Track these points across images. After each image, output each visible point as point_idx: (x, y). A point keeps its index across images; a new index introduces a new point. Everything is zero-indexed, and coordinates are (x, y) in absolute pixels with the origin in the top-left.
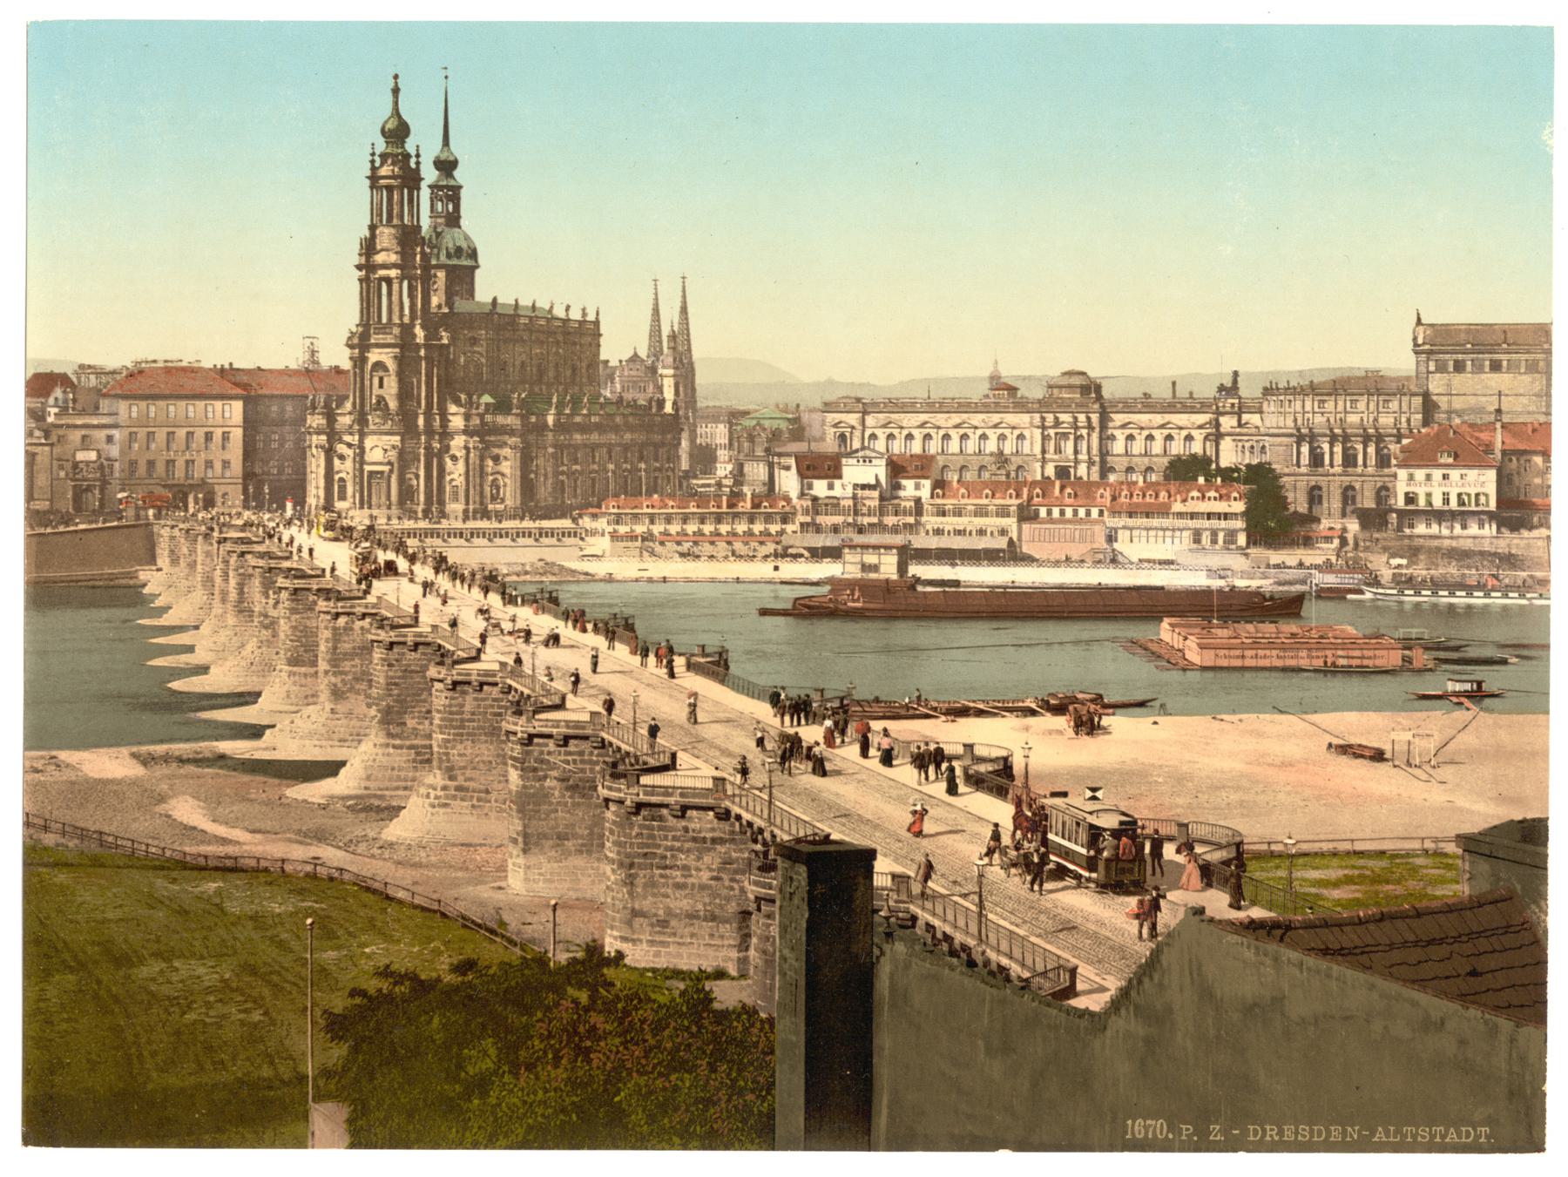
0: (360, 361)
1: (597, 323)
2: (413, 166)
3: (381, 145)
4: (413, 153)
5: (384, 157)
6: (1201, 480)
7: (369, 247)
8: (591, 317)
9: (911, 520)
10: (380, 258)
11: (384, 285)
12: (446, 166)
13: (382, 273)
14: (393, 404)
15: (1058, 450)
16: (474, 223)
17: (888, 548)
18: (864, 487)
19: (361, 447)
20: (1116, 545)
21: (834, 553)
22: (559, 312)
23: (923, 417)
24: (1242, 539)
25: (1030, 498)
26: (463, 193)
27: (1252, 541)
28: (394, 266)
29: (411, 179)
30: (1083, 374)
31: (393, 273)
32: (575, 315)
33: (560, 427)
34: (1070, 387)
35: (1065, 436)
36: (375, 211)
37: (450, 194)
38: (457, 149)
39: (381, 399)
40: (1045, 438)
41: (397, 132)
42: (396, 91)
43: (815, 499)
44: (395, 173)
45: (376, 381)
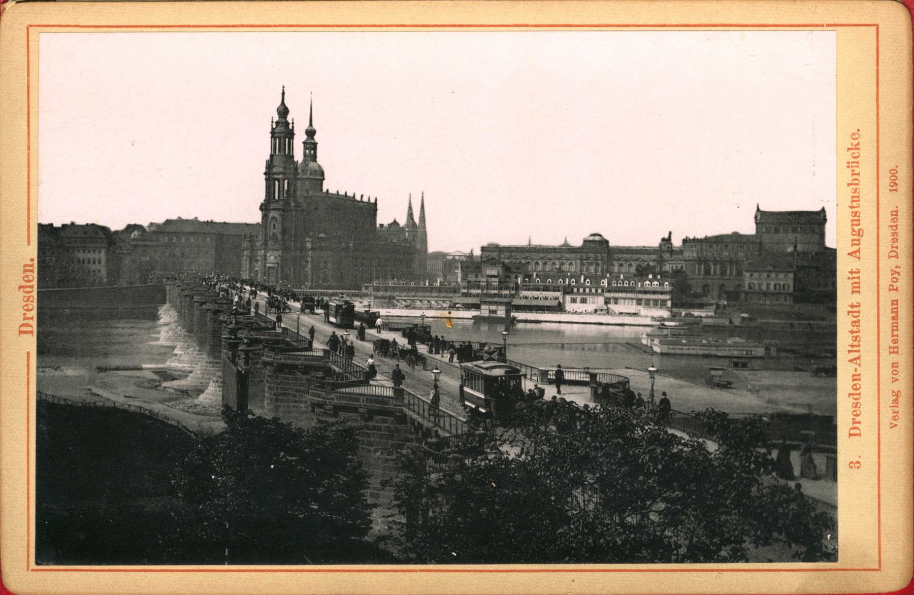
0: (265, 217)
1: (375, 204)
2: (290, 127)
3: (276, 118)
4: (290, 122)
5: (277, 123)
6: (650, 276)
7: (270, 165)
8: (372, 201)
9: (513, 292)
10: (275, 170)
11: (277, 183)
12: (311, 133)
13: (276, 176)
14: (280, 237)
15: (588, 269)
16: (323, 159)
17: (501, 303)
18: (492, 276)
19: (265, 256)
20: (609, 306)
21: (477, 307)
22: (358, 198)
23: (527, 254)
24: (669, 304)
25: (570, 284)
26: (318, 146)
27: (674, 305)
28: (281, 173)
29: (291, 134)
30: (600, 235)
31: (281, 176)
32: (365, 199)
33: (356, 249)
34: (594, 241)
35: (591, 264)
36: (274, 148)
37: (311, 146)
38: (315, 126)
39: (274, 234)
40: (582, 264)
41: (283, 111)
42: (283, 94)
43: (469, 282)
44: (282, 132)
45: (272, 226)
